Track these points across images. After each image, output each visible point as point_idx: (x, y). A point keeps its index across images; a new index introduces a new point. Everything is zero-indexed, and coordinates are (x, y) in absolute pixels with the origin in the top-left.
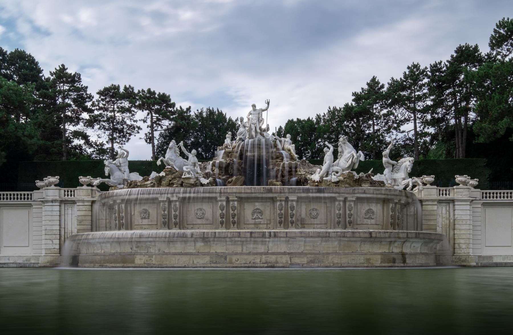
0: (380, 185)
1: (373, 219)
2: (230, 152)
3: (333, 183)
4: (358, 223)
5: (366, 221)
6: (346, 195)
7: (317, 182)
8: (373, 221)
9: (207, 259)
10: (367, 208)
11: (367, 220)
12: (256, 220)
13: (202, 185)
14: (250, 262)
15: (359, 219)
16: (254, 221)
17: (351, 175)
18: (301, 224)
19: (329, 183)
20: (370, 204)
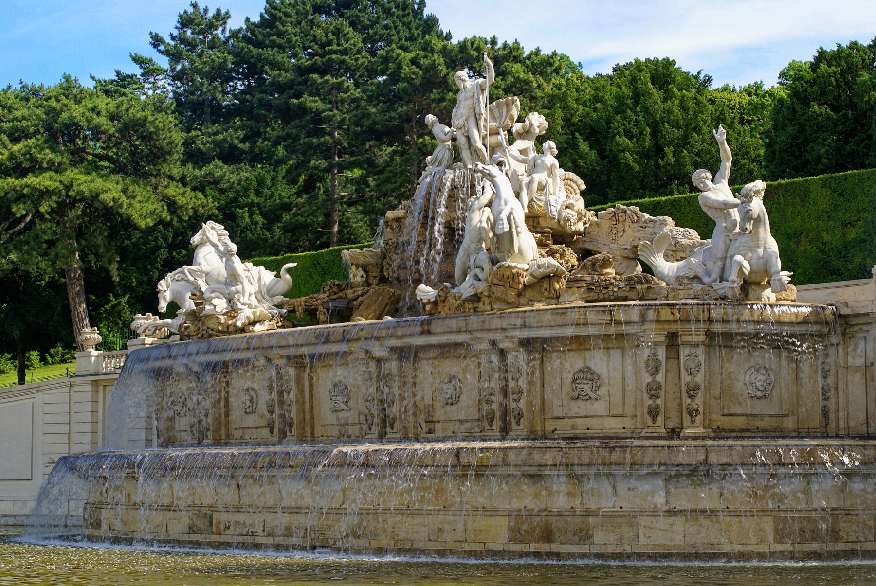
0: (632, 288)
1: (596, 399)
2: (398, 220)
3: (467, 300)
4: (556, 414)
5: (578, 408)
6: (491, 336)
7: (429, 302)
8: (599, 407)
9: (185, 519)
10: (579, 365)
11: (580, 403)
12: (341, 415)
13: (243, 330)
14: (248, 532)
15: (557, 402)
16: (335, 415)
17: (507, 273)
18: (426, 422)
19: (458, 302)
20: (588, 354)
